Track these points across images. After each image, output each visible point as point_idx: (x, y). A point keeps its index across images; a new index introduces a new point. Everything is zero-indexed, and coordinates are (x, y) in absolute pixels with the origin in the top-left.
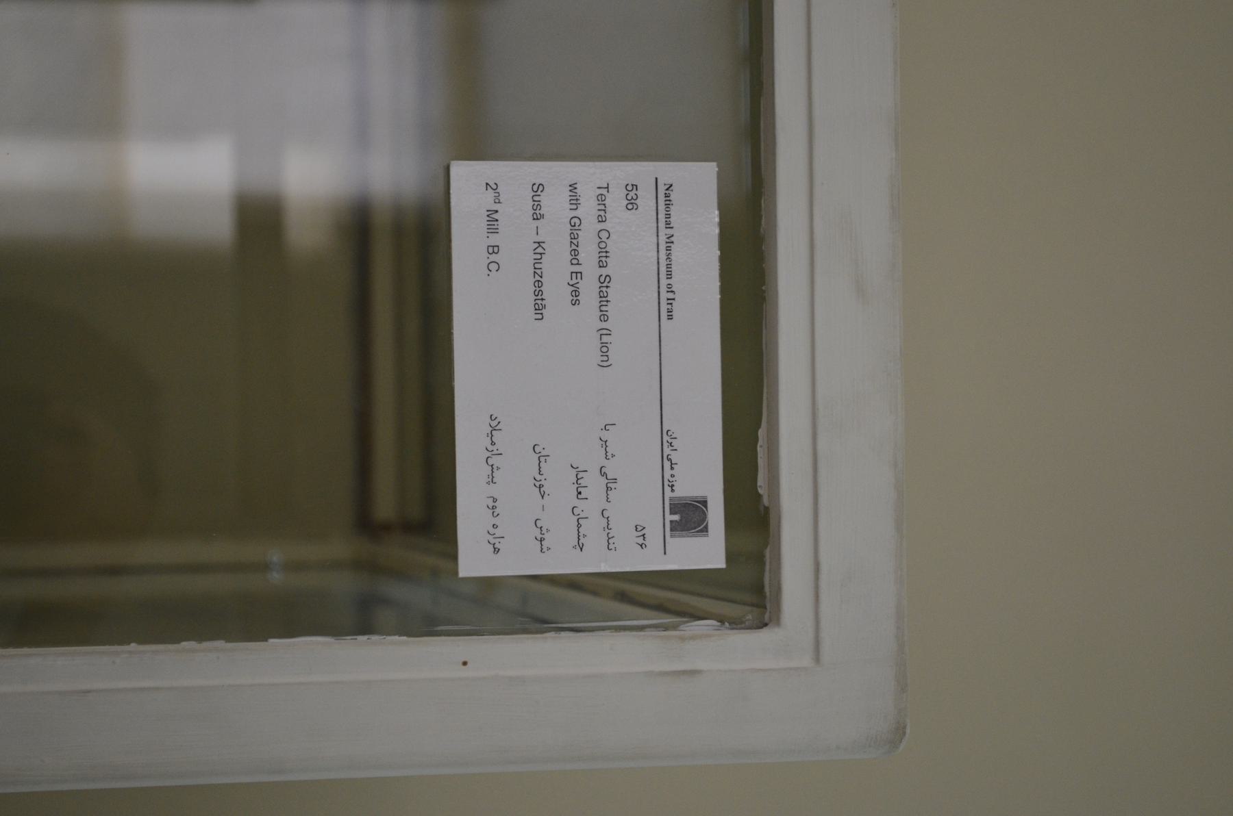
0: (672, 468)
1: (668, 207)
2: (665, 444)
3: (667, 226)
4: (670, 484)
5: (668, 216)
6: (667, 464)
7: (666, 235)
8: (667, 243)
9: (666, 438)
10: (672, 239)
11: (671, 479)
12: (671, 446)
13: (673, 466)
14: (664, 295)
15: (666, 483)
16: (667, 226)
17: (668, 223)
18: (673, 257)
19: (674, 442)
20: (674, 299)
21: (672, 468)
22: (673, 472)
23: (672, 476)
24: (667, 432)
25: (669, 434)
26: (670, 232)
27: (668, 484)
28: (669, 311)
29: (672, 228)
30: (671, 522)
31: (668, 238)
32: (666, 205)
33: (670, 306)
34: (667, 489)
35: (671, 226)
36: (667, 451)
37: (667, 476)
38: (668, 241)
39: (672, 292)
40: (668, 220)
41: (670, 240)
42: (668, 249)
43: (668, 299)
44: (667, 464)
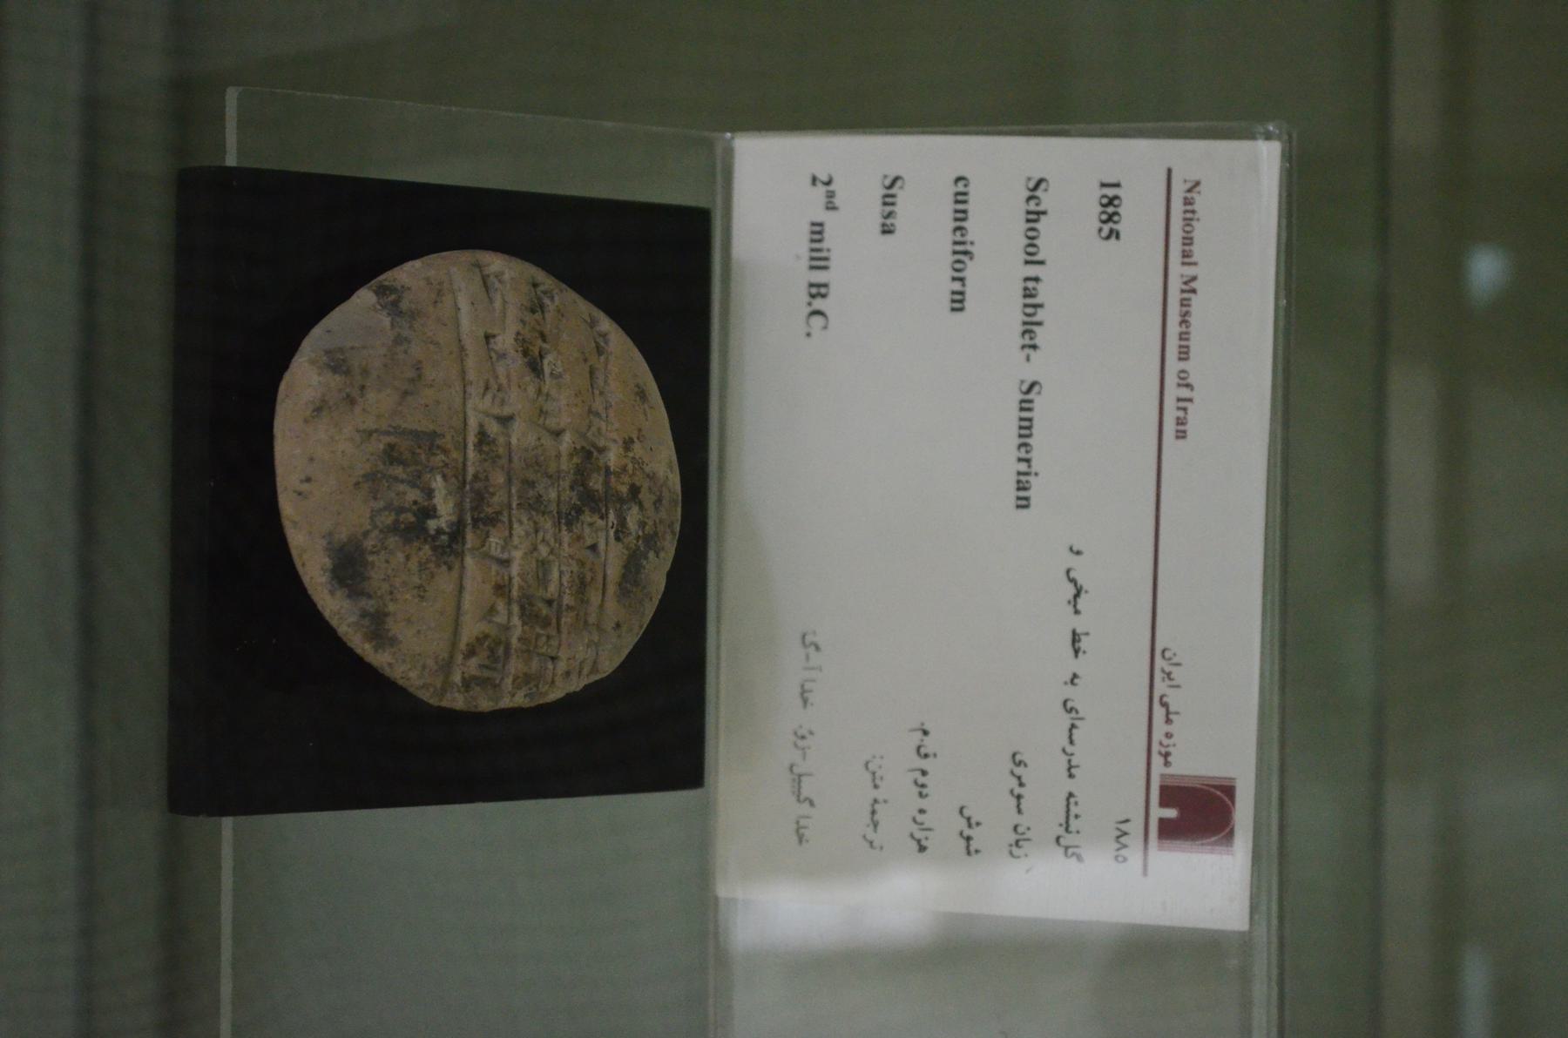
0: (1168, 721)
1: (1188, 225)
2: (1158, 675)
3: (1187, 260)
4: (1163, 750)
5: (1188, 241)
6: (1159, 712)
7: (1182, 276)
8: (1183, 291)
9: (1159, 662)
10: (1193, 285)
11: (1166, 742)
12: (1170, 679)
13: (1171, 717)
14: (1172, 392)
15: (1155, 748)
16: (1187, 260)
18: (1192, 320)
19: (1175, 671)
20: (1190, 400)
21: (1168, 721)
23: (1168, 735)
24: (1163, 651)
25: (1167, 654)
26: (1190, 271)
28: (1180, 422)
30: (1163, 823)
31: (1185, 283)
32: (1185, 219)
33: (1181, 414)
34: (1157, 761)
36: (1160, 687)
37: (1158, 735)
38: (1184, 287)
39: (1188, 386)
40: (1187, 248)
41: (1189, 286)
42: (1184, 303)
43: (1179, 400)
44: (1159, 712)
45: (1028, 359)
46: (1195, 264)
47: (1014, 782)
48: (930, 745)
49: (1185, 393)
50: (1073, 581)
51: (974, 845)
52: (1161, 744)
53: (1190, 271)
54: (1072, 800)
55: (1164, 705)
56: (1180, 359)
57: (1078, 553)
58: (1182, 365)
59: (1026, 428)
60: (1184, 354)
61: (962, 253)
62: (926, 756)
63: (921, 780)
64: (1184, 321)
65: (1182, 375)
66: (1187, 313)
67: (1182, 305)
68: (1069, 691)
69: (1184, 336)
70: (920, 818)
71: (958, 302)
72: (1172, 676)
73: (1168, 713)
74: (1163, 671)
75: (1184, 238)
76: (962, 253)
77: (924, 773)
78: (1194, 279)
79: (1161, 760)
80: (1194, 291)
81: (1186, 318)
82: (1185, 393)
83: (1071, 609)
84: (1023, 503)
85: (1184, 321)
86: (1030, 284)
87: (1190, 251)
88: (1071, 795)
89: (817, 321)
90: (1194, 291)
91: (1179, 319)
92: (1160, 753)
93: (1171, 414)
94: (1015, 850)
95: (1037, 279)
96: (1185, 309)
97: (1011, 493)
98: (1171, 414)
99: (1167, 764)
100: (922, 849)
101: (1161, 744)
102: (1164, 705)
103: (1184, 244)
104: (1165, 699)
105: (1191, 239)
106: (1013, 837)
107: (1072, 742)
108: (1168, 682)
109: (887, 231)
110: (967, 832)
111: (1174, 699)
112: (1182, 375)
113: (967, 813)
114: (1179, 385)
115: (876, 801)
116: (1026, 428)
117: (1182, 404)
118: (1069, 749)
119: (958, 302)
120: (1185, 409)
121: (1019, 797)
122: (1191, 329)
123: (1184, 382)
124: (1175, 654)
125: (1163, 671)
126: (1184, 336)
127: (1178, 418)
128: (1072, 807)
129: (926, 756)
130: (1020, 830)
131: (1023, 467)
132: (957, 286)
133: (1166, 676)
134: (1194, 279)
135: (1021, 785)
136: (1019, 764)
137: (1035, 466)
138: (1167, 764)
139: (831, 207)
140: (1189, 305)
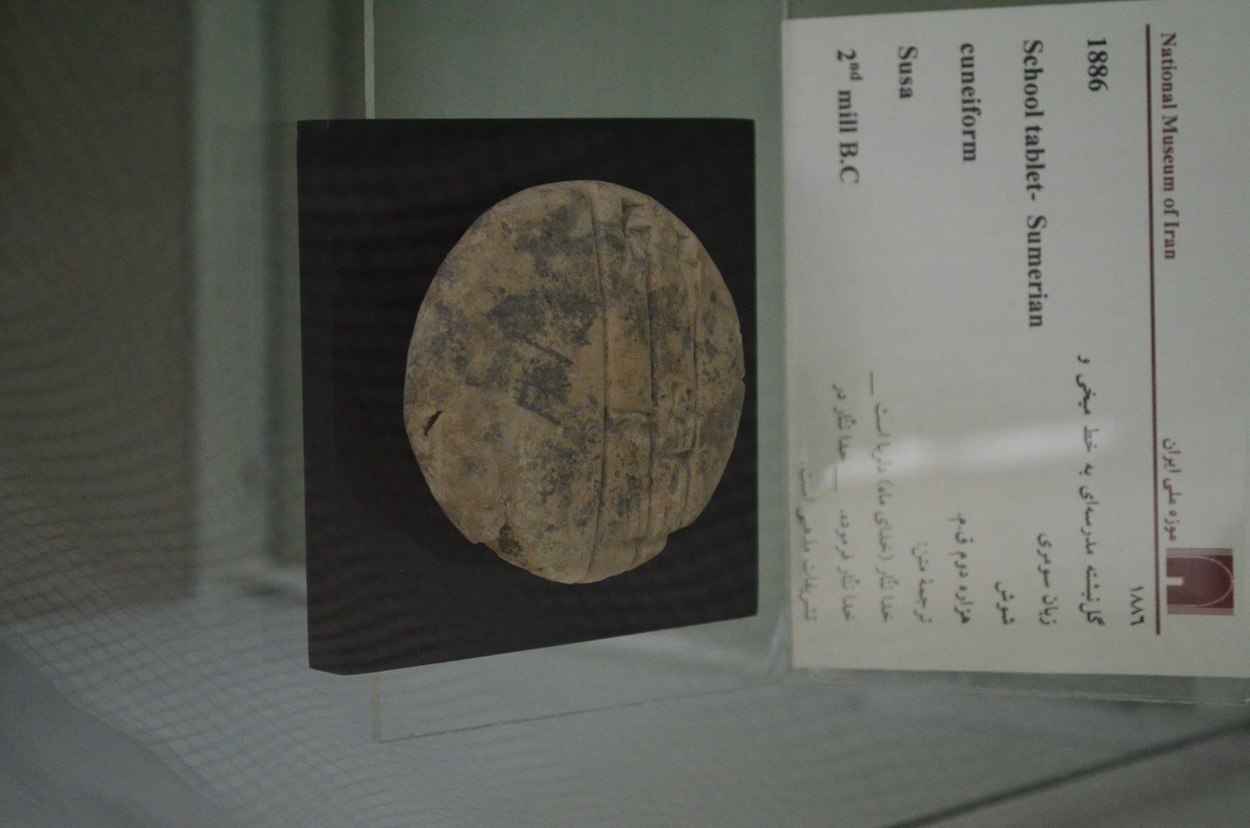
2: (1161, 463)
3: (1167, 104)
4: (1169, 527)
5: (1167, 86)
6: (1163, 495)
7: (1164, 118)
8: (1165, 131)
9: (1161, 451)
10: (1174, 124)
11: (1170, 519)
13: (1174, 497)
14: (1160, 218)
15: (1161, 524)
16: (1167, 104)
17: (1166, 99)
18: (1174, 154)
21: (1171, 501)
22: (1172, 507)
23: (1172, 513)
24: (1164, 442)
25: (1168, 444)
26: (1170, 113)
27: (1161, 526)
28: (1168, 243)
29: (1175, 106)
30: (1171, 591)
31: (1167, 123)
33: (1169, 237)
34: (1164, 536)
35: (1172, 103)
36: (1163, 473)
38: (1167, 127)
40: (1167, 93)
41: (1170, 127)
42: (1167, 141)
43: (1167, 225)
44: (1163, 495)
45: (1033, 197)
46: (1175, 106)
47: (1041, 560)
48: (967, 532)
49: (1171, 218)
50: (1082, 385)
51: (1009, 615)
52: (1166, 520)
53: (1170, 113)
54: (1092, 573)
55: (1168, 487)
56: (1166, 189)
57: (1086, 361)
58: (1168, 195)
59: (1035, 257)
60: (1169, 184)
61: (971, 109)
62: (964, 541)
63: (961, 562)
64: (1168, 156)
65: (1168, 203)
66: (1169, 150)
67: (1165, 143)
68: (1084, 481)
69: (1168, 169)
70: (961, 594)
71: (970, 153)
72: (1173, 463)
73: (1171, 494)
74: (1165, 458)
75: (1164, 85)
76: (971, 109)
77: (963, 556)
78: (1175, 119)
79: (1167, 534)
80: (1175, 130)
81: (1170, 154)
82: (1171, 218)
83: (1082, 409)
84: (1036, 322)
85: (1168, 156)
86: (1032, 133)
87: (1170, 95)
88: (1090, 568)
89: (849, 176)
90: (1175, 130)
91: (1163, 155)
92: (1166, 529)
93: (1160, 238)
94: (1046, 618)
95: (1037, 129)
96: (1167, 146)
97: (1024, 314)
98: (1160, 238)
99: (1172, 538)
100: (965, 620)
101: (1166, 520)
102: (1168, 487)
103: (1164, 90)
104: (1168, 483)
105: (1170, 85)
106: (1042, 607)
107: (1088, 523)
108: (1169, 468)
109: (905, 94)
110: (1003, 604)
111: (1175, 481)
112: (1168, 203)
113: (1001, 588)
114: (1166, 212)
115: (923, 581)
116: (1035, 257)
117: (1169, 228)
118: (1087, 529)
119: (970, 153)
120: (1172, 232)
121: (1046, 573)
122: (1175, 163)
123: (1170, 209)
124: (1174, 444)
125: (1165, 458)
126: (1168, 169)
127: (1167, 241)
128: (1092, 578)
129: (964, 541)
130: (1048, 600)
131: (1034, 290)
132: (968, 139)
133: (1167, 463)
134: (1175, 119)
135: (1047, 562)
136: (1045, 544)
137: (1045, 290)
138: (1172, 538)
139: (855, 77)
140: (1171, 143)
